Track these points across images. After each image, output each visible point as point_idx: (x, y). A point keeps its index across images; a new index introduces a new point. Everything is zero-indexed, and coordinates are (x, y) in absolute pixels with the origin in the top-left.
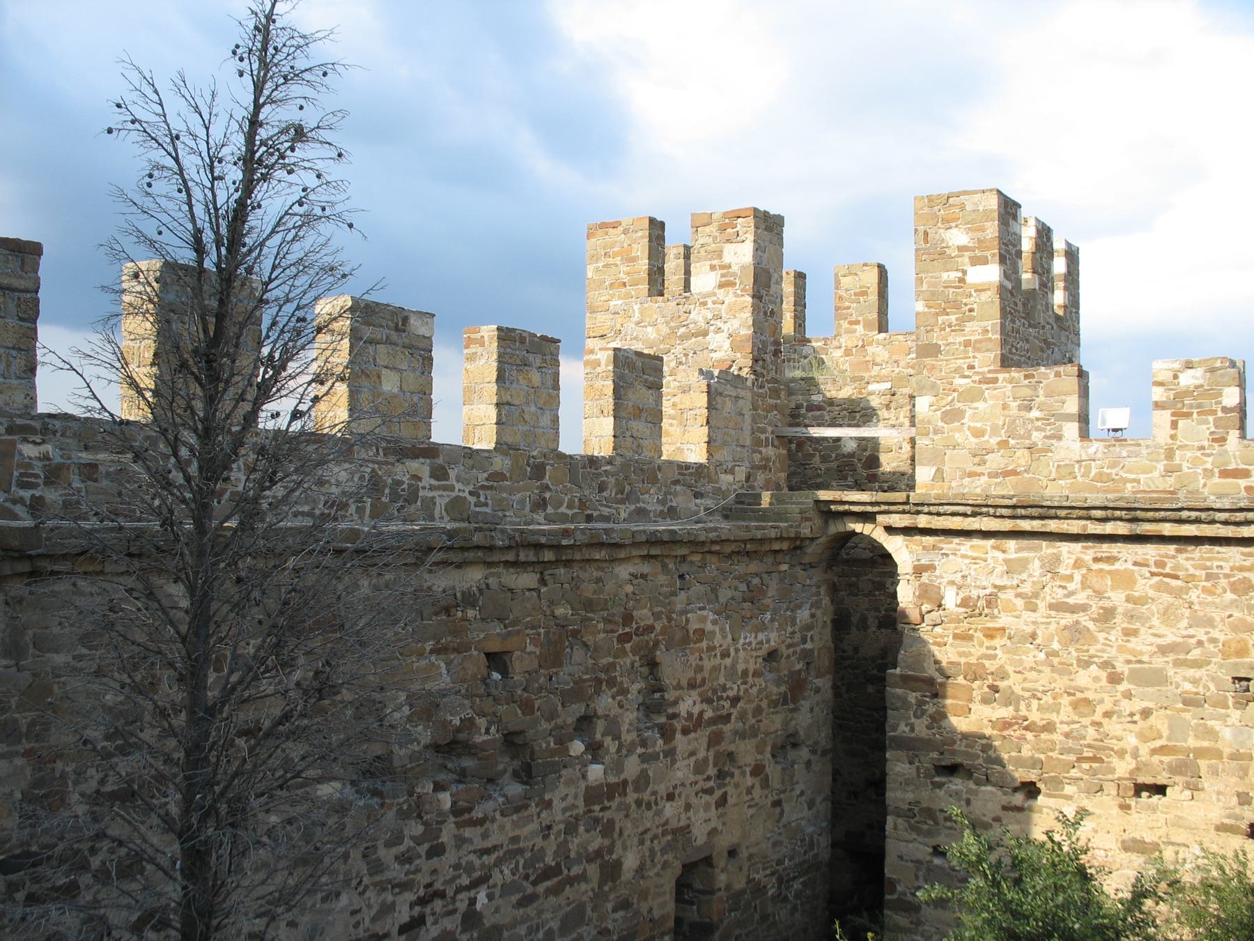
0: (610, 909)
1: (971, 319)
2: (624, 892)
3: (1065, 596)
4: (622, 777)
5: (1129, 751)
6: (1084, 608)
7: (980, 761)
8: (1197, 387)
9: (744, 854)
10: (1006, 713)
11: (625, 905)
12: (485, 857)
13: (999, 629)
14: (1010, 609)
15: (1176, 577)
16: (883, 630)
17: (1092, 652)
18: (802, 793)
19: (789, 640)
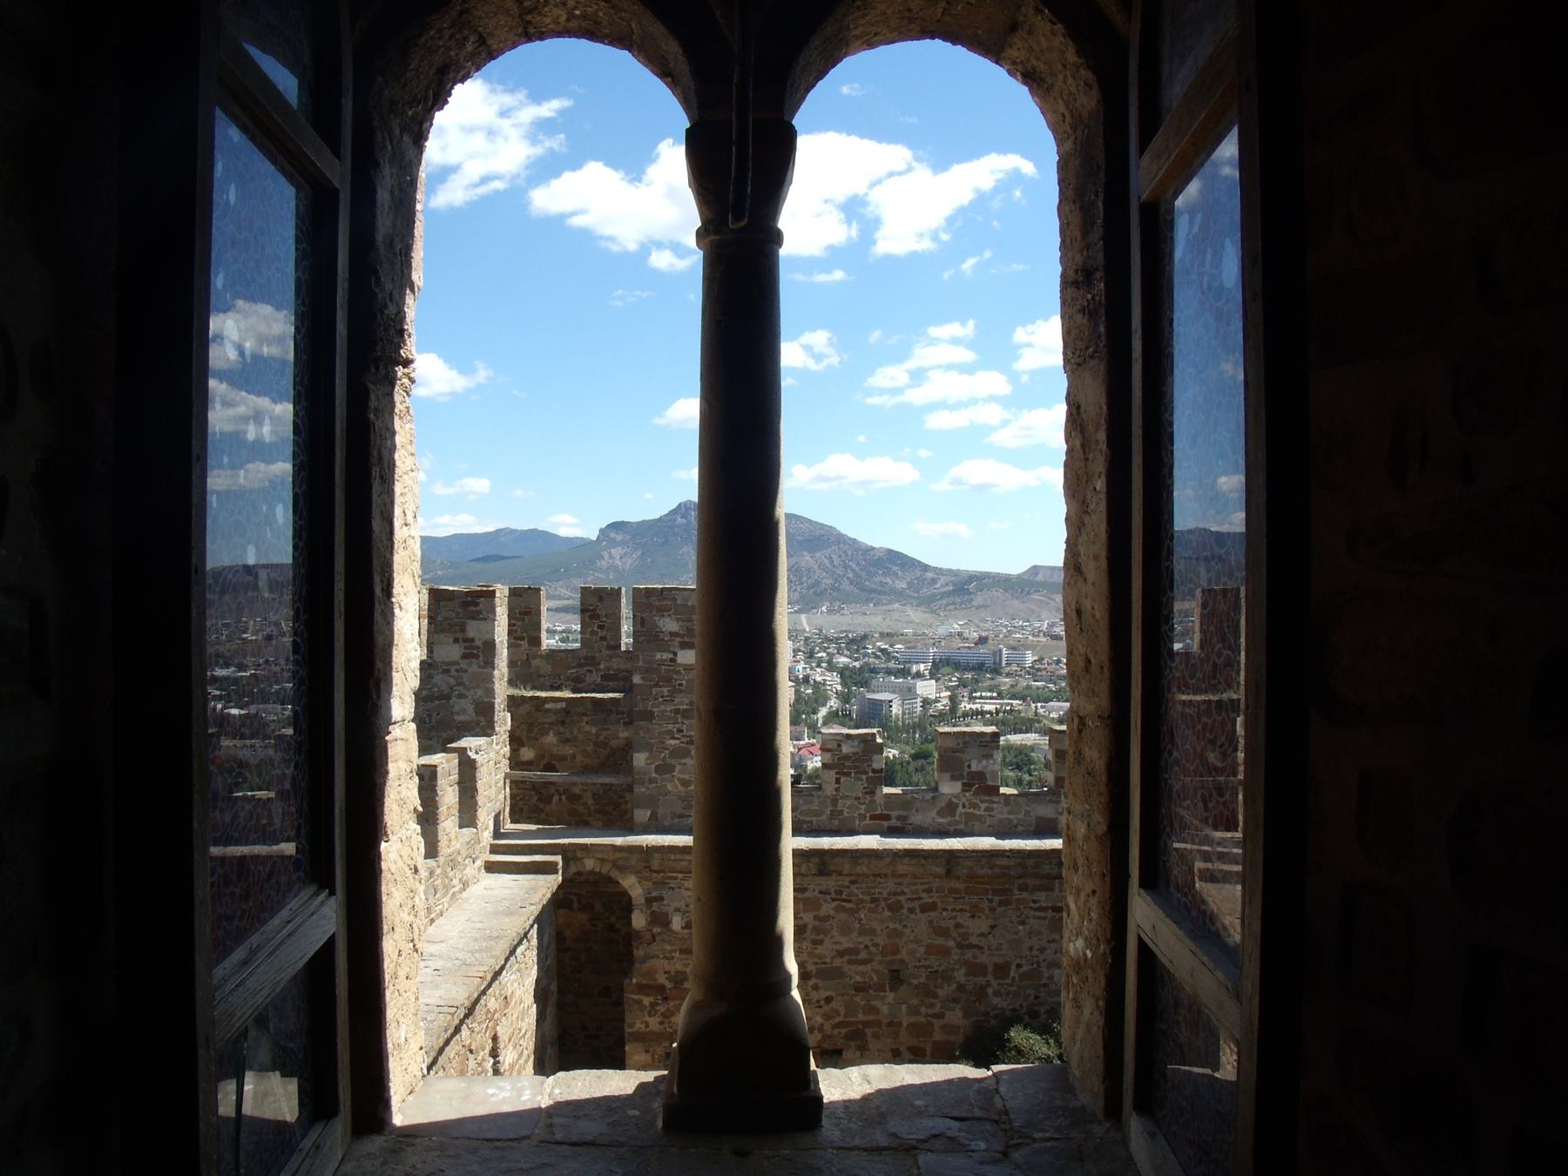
1: (681, 691)
5: (817, 1027)
8: (854, 754)
15: (850, 901)
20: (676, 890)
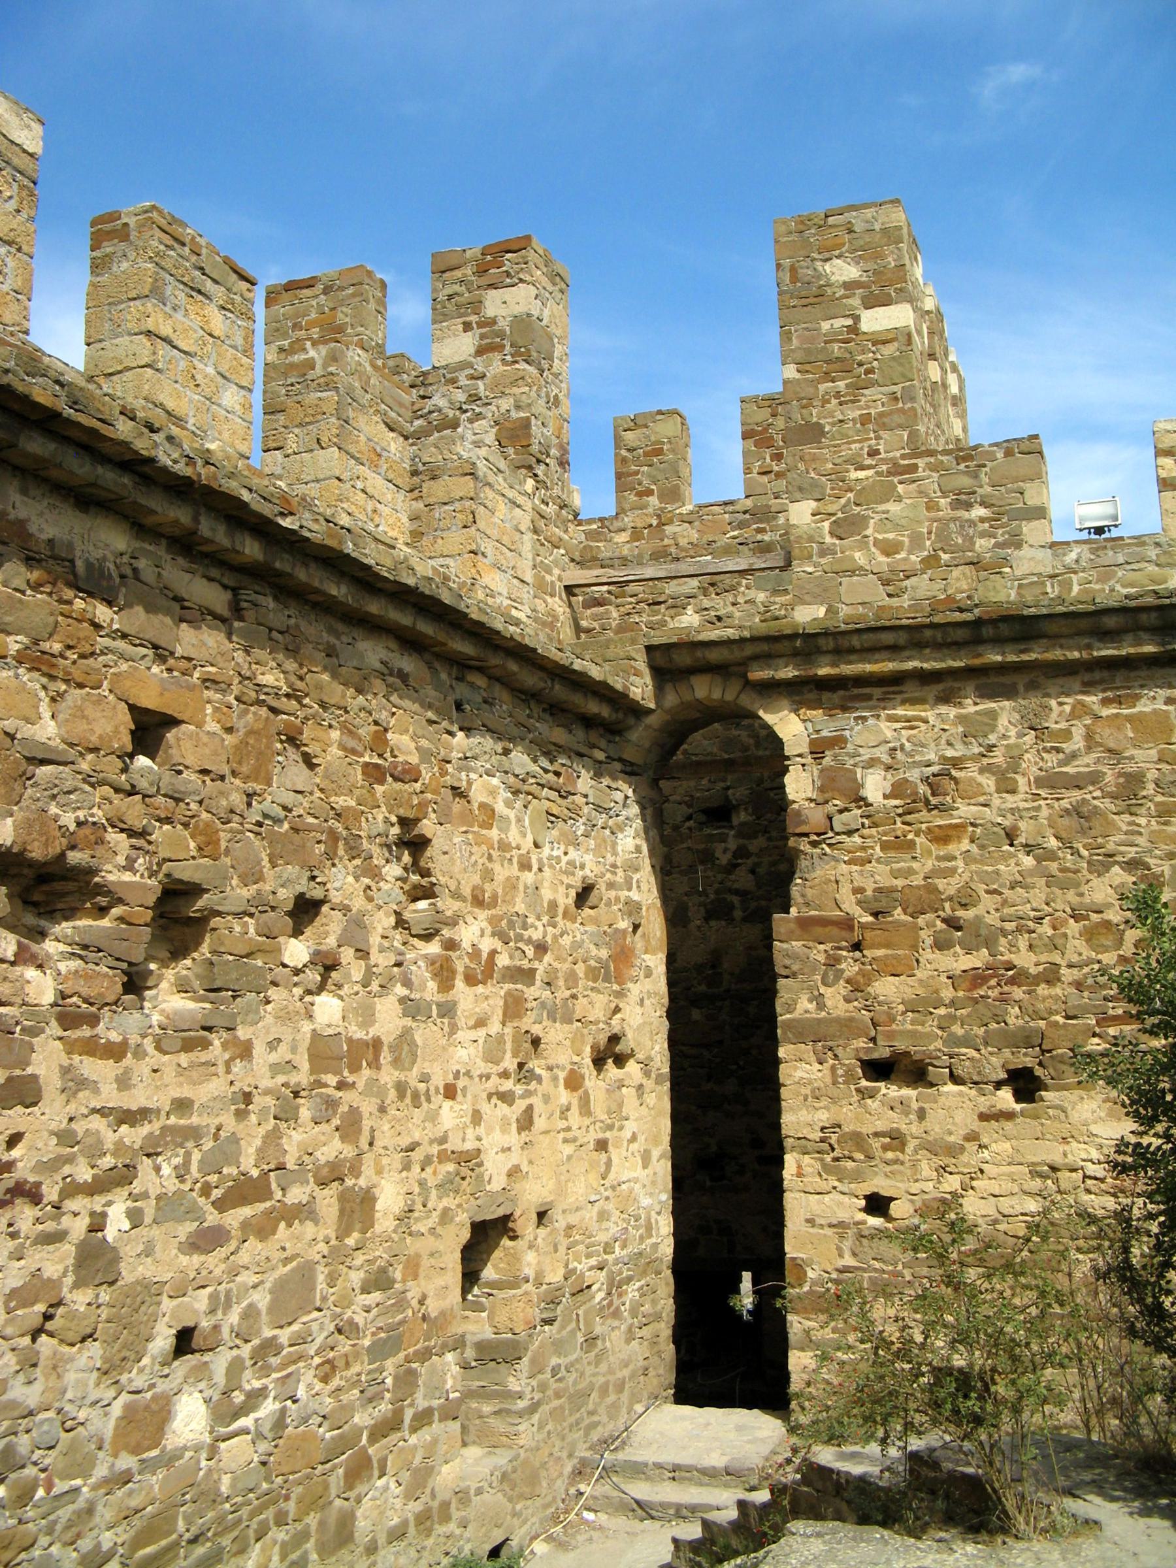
0: (357, 1285)
2: (380, 1252)
3: (1062, 763)
4: (373, 1032)
6: (1094, 778)
7: (939, 1044)
9: (559, 1220)
10: (978, 959)
11: (379, 1281)
12: (124, 1128)
13: (956, 826)
14: (971, 794)
16: (713, 923)
17: (1111, 847)
18: (634, 1138)
19: (608, 875)
20: (871, 721)
